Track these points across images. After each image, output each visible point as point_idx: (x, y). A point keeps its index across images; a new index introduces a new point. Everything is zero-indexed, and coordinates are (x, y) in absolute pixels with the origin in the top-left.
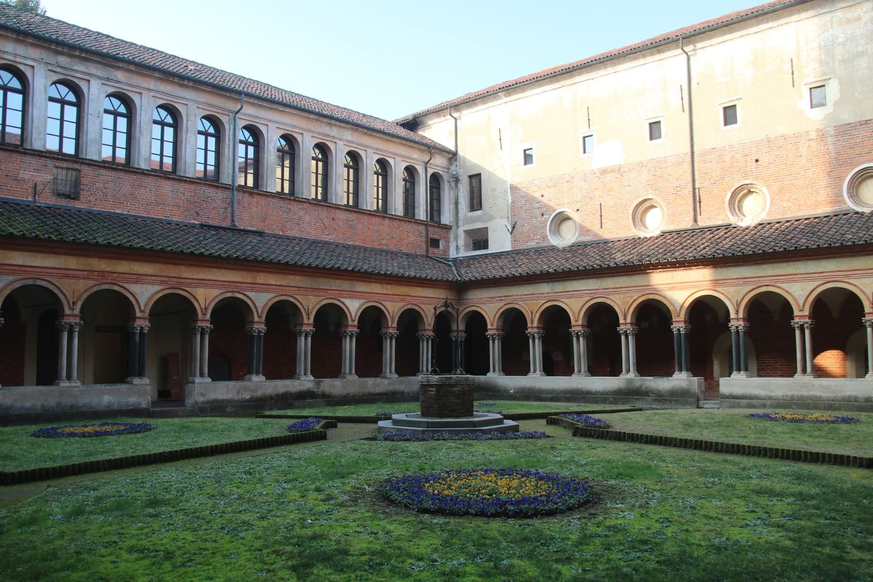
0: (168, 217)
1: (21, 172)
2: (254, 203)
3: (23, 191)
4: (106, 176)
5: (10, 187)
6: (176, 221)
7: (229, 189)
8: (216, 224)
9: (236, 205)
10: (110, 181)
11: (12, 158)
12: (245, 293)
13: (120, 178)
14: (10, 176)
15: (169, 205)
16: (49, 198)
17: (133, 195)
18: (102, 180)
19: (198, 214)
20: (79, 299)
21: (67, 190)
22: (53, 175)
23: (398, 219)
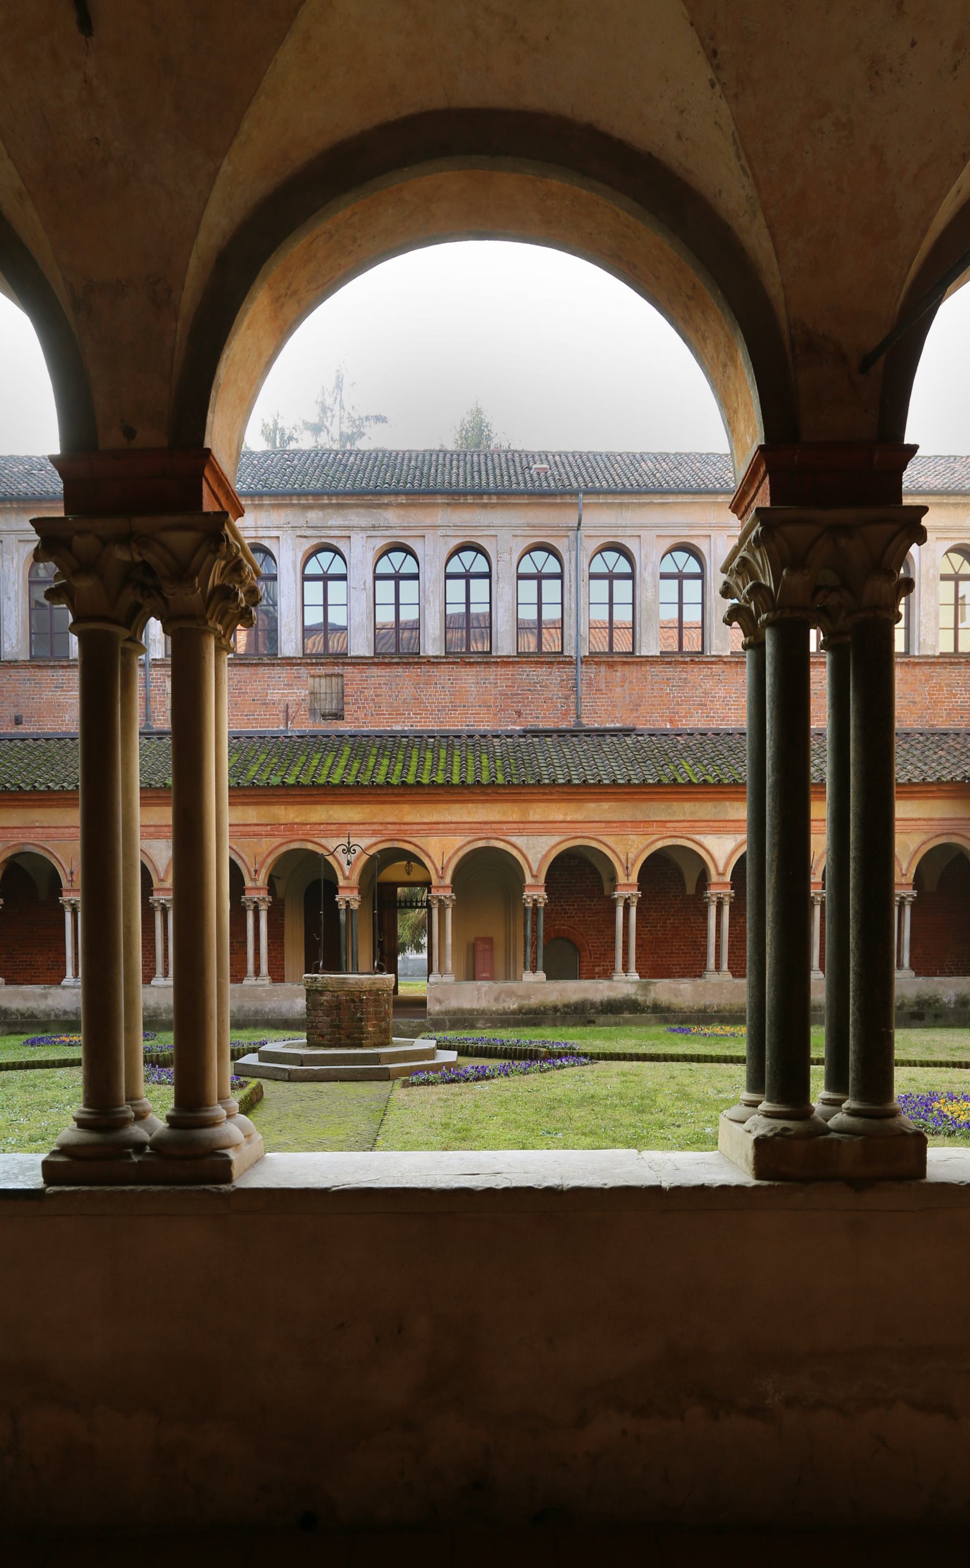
0: (472, 726)
1: (269, 691)
2: (618, 680)
3: (273, 719)
4: (378, 676)
5: (258, 715)
6: (468, 731)
7: (570, 663)
8: (550, 726)
9: (583, 688)
10: (384, 684)
11: (258, 674)
12: (509, 838)
13: (397, 676)
14: (258, 700)
15: (474, 706)
16: (304, 723)
17: (418, 699)
18: (372, 684)
19: (519, 713)
20: (262, 866)
21: (330, 706)
22: (307, 689)
23: (926, 663)
